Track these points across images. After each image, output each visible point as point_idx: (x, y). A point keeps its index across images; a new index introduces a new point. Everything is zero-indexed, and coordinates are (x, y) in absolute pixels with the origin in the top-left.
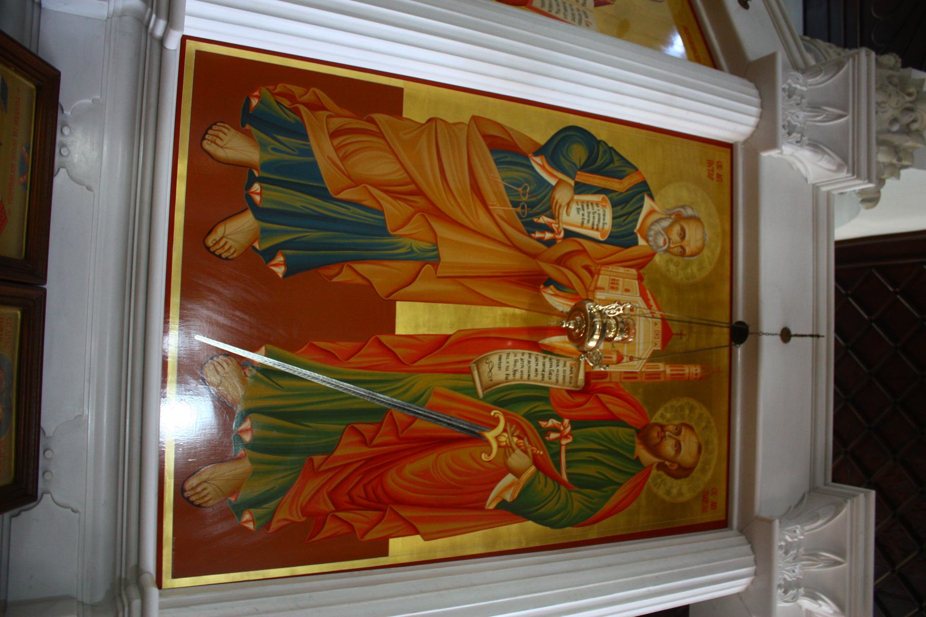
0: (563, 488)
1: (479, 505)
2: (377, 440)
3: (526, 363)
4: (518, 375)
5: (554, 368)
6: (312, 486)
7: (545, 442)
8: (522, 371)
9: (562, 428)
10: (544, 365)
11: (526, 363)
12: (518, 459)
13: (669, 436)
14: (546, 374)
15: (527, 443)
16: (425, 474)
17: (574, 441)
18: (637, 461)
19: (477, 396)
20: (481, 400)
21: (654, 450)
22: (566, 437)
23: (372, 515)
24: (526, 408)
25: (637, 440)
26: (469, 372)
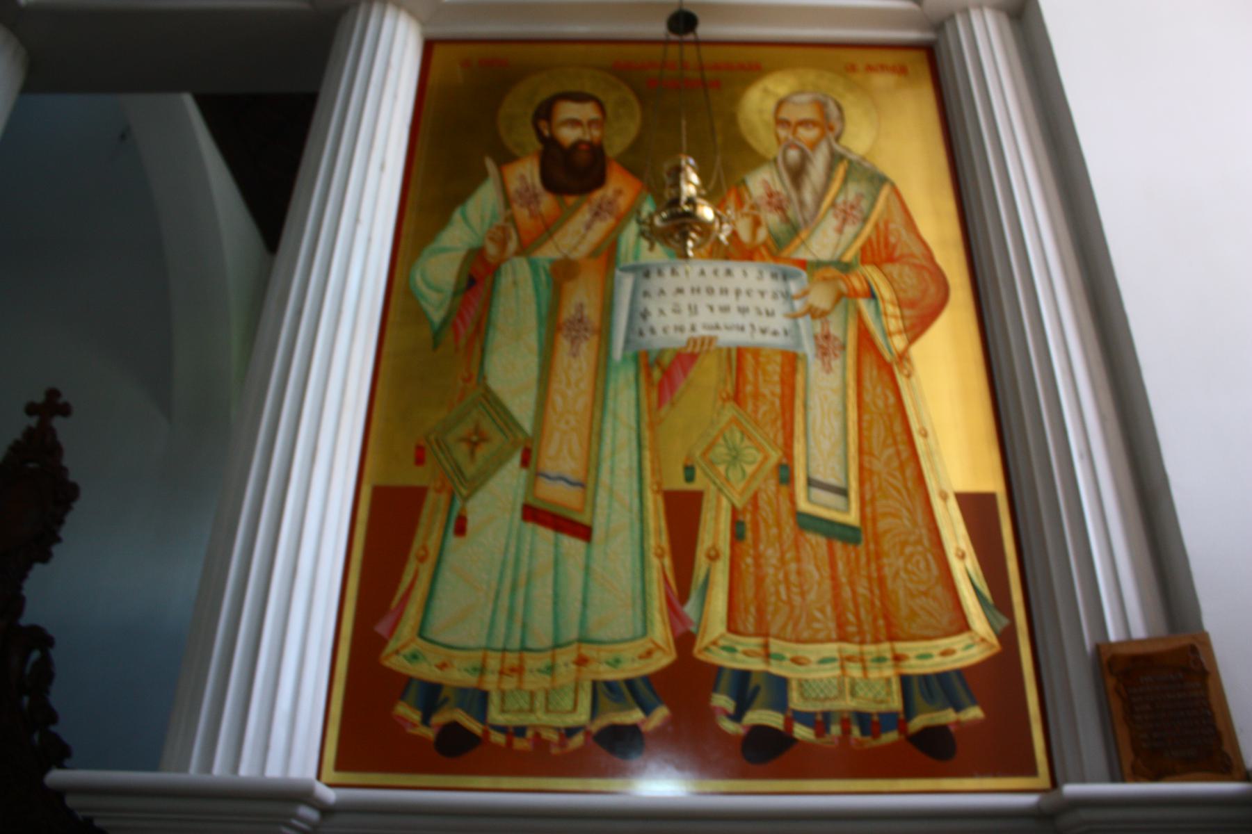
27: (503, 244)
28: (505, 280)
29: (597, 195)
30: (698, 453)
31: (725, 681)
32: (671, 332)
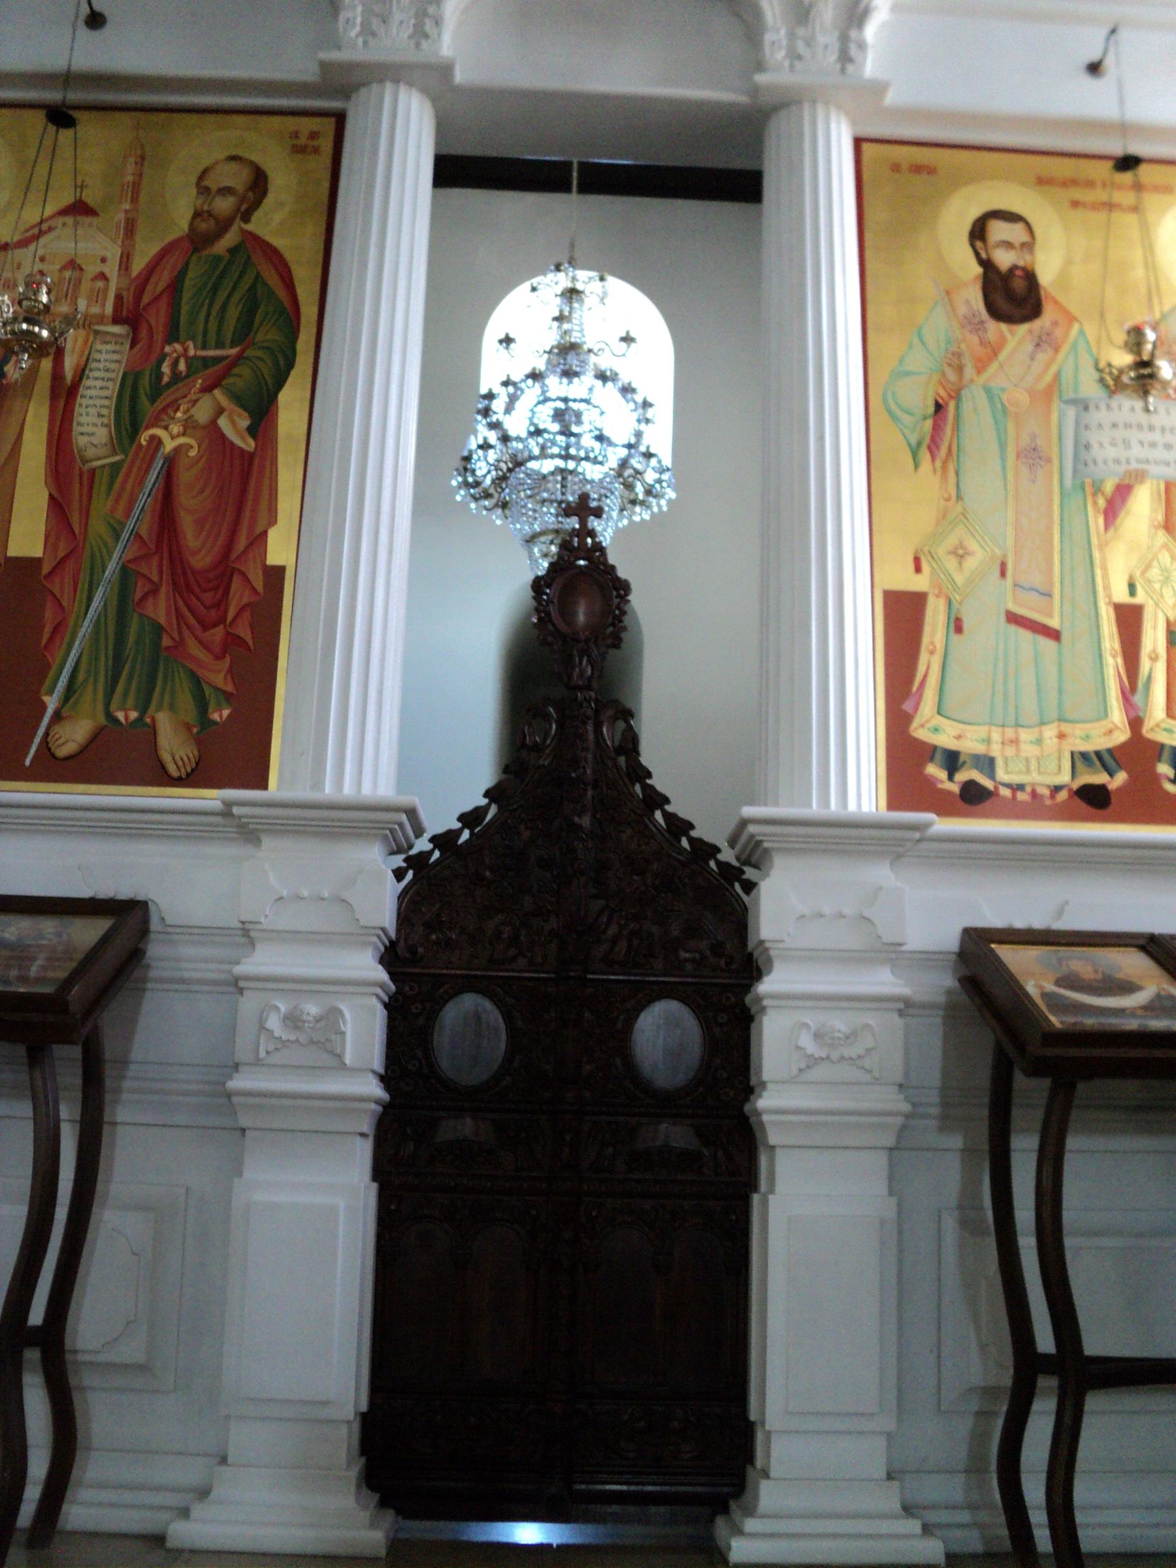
0: (249, 353)
1: (248, 458)
2: (155, 578)
3: (91, 402)
4: (105, 412)
5: (101, 366)
6: (194, 648)
7: (188, 376)
8: (101, 407)
9: (175, 355)
10: (97, 379)
11: (91, 402)
12: (202, 412)
13: (210, 204)
14: (108, 375)
15: (185, 400)
16: (200, 523)
17: (193, 339)
18: (233, 251)
19: (123, 461)
20: (126, 456)
21: (224, 226)
22: (186, 350)
23: (236, 582)
24: (144, 400)
25: (205, 253)
26: (93, 472)
27: (960, 369)
28: (967, 406)
29: (1037, 324)
30: (1138, 574)
31: (1166, 755)
32: (1110, 463)
